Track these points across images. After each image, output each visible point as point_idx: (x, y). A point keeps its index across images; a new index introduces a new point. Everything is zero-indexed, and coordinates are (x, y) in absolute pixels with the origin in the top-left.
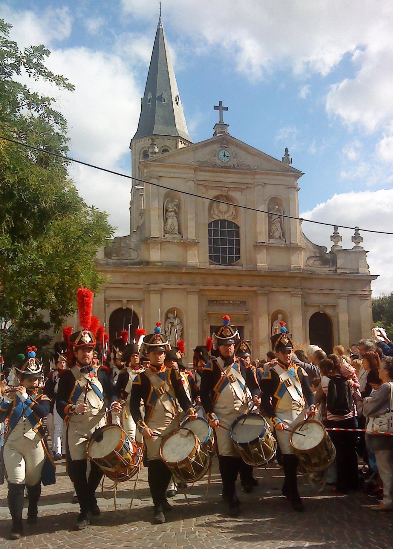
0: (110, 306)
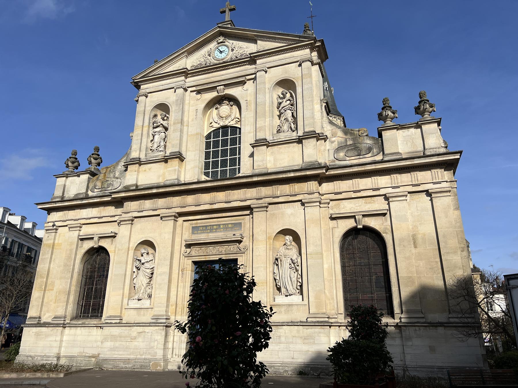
0: (84, 246)
